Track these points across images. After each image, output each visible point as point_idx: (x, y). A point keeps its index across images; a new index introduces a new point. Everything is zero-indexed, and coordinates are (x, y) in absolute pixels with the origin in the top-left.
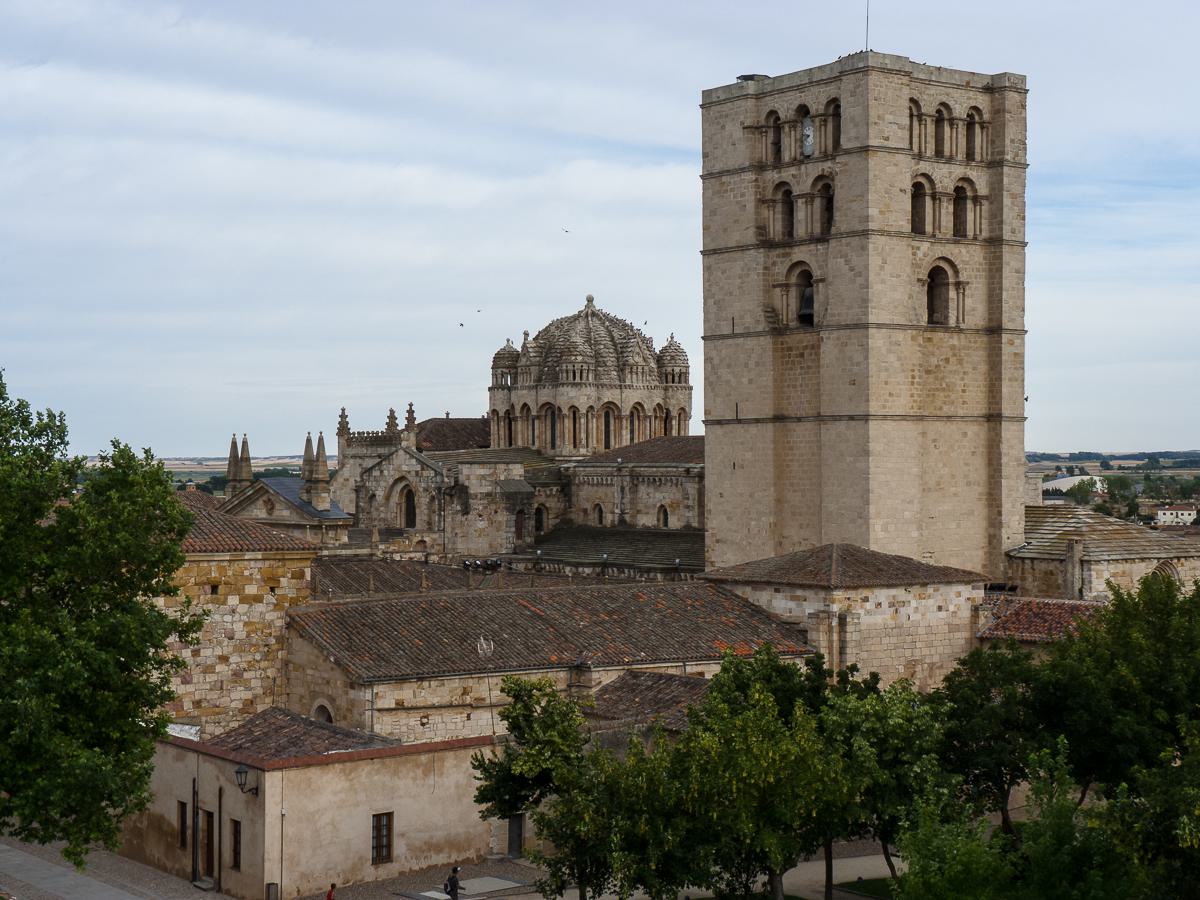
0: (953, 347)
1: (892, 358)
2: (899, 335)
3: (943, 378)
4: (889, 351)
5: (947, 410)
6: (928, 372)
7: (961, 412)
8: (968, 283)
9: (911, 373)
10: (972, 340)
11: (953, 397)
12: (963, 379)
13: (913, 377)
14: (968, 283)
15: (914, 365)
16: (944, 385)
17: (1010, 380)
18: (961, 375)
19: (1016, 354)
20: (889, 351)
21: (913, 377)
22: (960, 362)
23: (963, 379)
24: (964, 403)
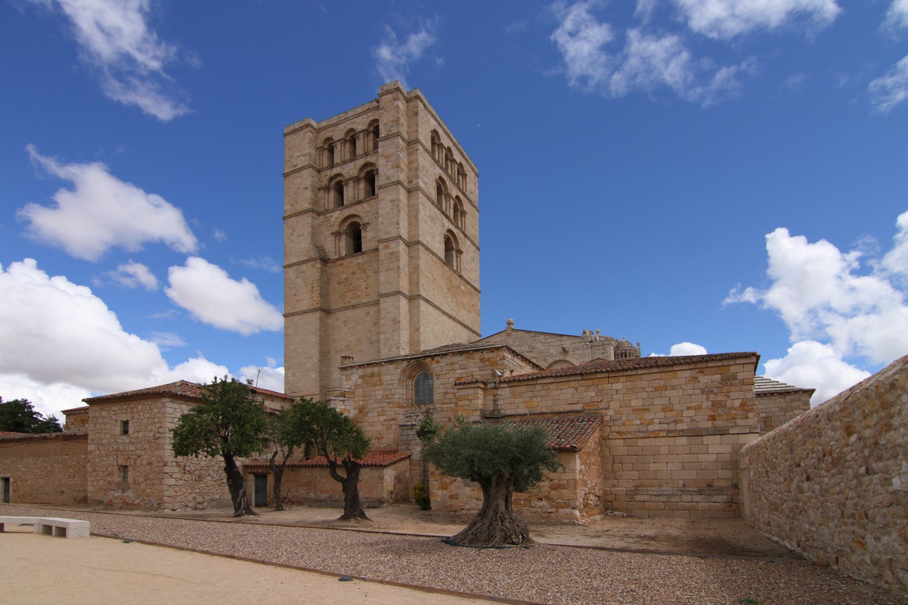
0: (358, 264)
1: (299, 281)
2: (304, 267)
3: (351, 284)
4: (297, 278)
5: (353, 302)
6: (339, 283)
7: (364, 301)
8: (368, 223)
9: (310, 287)
10: (373, 256)
11: (359, 293)
12: (366, 281)
13: (313, 287)
14: (368, 223)
15: (313, 281)
16: (352, 288)
17: (386, 271)
18: (365, 278)
19: (391, 254)
20: (297, 278)
21: (313, 287)
22: (364, 271)
23: (366, 281)
24: (367, 295)
